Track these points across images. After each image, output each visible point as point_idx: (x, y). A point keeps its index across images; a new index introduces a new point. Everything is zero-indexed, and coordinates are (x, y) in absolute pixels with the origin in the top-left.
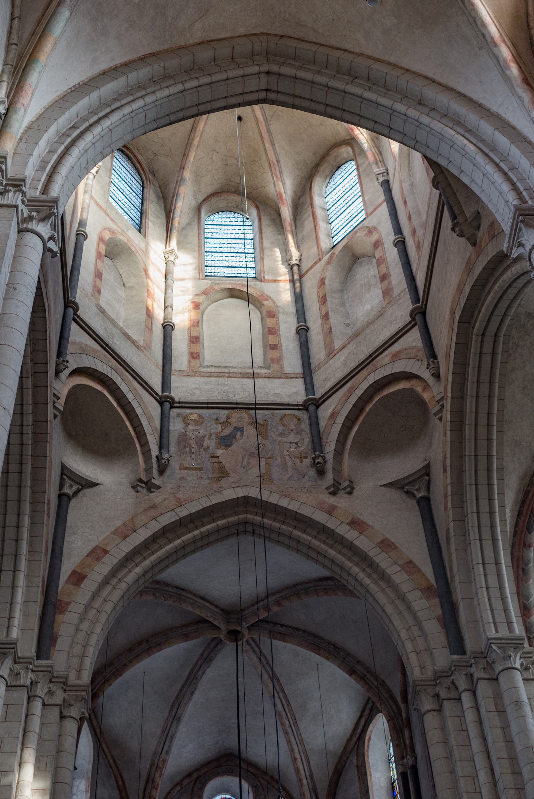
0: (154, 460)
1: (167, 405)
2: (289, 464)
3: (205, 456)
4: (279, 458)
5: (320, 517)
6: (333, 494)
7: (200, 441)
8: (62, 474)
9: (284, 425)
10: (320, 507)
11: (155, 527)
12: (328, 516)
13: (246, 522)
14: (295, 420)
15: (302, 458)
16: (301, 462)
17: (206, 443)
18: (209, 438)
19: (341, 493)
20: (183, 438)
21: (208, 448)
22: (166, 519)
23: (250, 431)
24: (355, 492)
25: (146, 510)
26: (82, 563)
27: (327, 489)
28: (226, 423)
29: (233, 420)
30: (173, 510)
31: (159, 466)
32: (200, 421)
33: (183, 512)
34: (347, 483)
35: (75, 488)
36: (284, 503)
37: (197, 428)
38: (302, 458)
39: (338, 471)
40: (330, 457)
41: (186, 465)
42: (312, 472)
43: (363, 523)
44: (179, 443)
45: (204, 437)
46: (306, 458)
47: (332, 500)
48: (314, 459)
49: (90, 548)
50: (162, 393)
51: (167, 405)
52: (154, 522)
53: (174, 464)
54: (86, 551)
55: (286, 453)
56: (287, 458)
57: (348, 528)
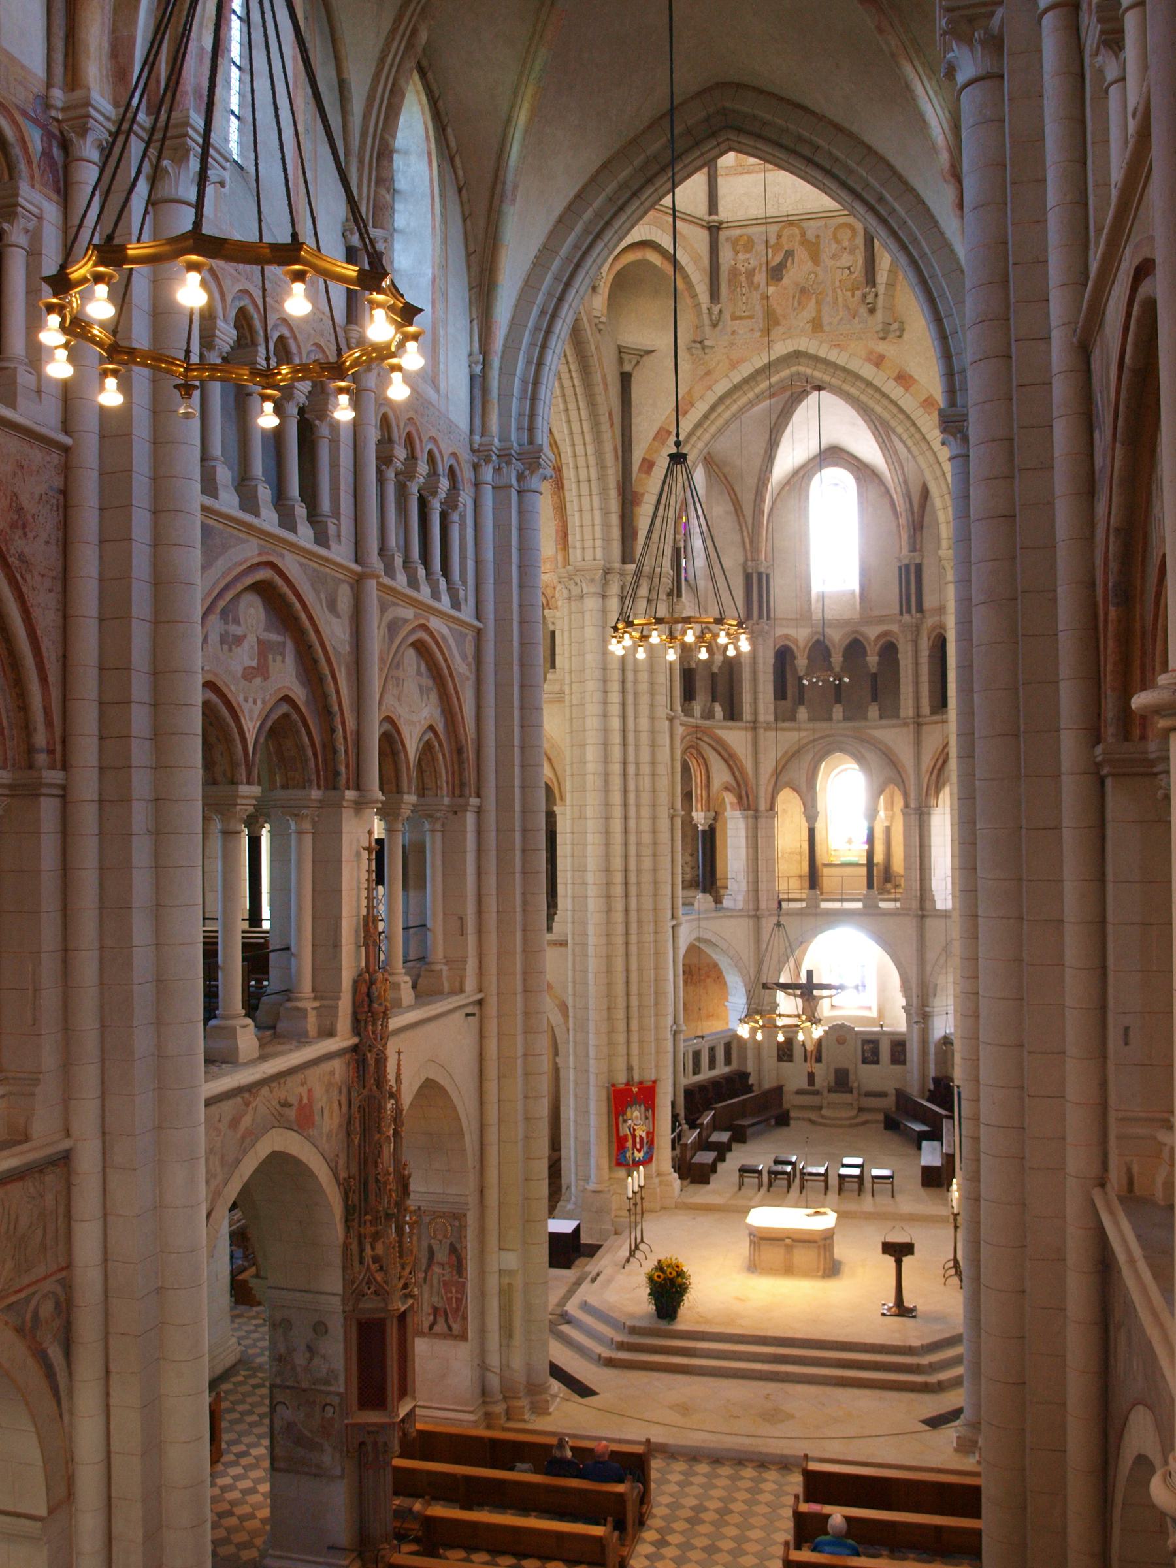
0: (705, 311)
1: (714, 230)
2: (840, 300)
3: (756, 296)
4: (830, 292)
5: (868, 371)
6: (883, 339)
7: (750, 274)
8: (620, 352)
9: (838, 242)
10: (869, 360)
11: (711, 398)
12: (875, 369)
13: (798, 374)
14: (849, 232)
15: (853, 290)
16: (853, 296)
17: (756, 279)
18: (760, 272)
19: (891, 336)
20: (734, 273)
21: (759, 285)
22: (722, 387)
23: (801, 254)
24: (906, 336)
25: (701, 378)
26: (650, 449)
27: (877, 332)
28: (777, 246)
29: (784, 240)
30: (727, 376)
31: (711, 320)
32: (749, 245)
33: (737, 378)
34: (895, 326)
35: (634, 362)
36: (833, 356)
37: (748, 256)
38: (853, 290)
39: (891, 308)
40: (881, 289)
41: (738, 314)
42: (863, 310)
43: (911, 377)
44: (730, 281)
45: (754, 269)
46: (858, 289)
47: (882, 347)
48: (865, 296)
49: (656, 429)
50: (710, 214)
51: (714, 230)
52: (709, 392)
53: (727, 315)
54: (652, 435)
55: (837, 283)
56: (839, 291)
57: (895, 384)
